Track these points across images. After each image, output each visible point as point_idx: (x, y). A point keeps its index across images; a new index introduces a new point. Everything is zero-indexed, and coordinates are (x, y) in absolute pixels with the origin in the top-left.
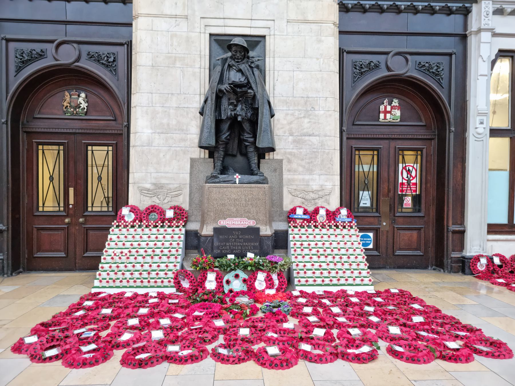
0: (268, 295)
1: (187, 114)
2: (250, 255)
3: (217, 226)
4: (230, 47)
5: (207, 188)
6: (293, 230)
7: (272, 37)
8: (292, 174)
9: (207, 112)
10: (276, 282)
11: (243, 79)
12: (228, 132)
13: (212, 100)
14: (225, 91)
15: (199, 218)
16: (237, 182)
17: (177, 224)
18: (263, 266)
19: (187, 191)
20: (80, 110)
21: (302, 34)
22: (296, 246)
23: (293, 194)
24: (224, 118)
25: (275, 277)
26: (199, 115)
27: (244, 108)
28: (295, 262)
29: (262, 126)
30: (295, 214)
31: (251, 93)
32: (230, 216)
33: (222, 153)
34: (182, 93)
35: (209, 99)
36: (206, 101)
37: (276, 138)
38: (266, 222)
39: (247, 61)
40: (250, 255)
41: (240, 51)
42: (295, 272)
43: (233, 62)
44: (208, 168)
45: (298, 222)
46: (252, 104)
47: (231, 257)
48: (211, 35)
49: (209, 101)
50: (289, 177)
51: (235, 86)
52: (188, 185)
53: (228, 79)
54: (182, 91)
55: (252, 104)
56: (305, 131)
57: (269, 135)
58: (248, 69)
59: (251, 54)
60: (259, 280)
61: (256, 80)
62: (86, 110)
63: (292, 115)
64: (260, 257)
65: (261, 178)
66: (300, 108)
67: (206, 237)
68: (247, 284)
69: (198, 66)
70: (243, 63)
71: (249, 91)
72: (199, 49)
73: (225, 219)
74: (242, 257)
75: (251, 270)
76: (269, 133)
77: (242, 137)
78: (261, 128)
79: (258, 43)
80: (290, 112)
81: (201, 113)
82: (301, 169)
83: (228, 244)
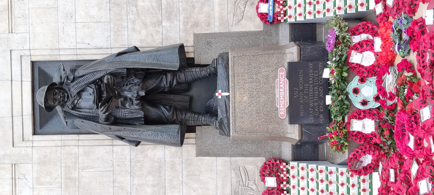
0: (383, 47)
1: (138, 161)
2: (326, 73)
3: (287, 119)
4: (49, 108)
5: (236, 135)
6: (290, 17)
7: (32, 52)
8: (212, 21)
9: (135, 136)
10: (364, 36)
11: (91, 90)
12: (160, 108)
13: (119, 130)
14: (107, 113)
15: (276, 143)
16: (227, 94)
17: (285, 173)
18: (341, 56)
19: (240, 160)
21: (27, 12)
22: (312, 11)
23: (240, 18)
24: (143, 113)
25: (356, 39)
26: (139, 147)
27: (128, 87)
28: (335, 12)
29: (151, 63)
30: (267, 14)
31: (108, 79)
32: (273, 101)
33: (189, 115)
34: (112, 169)
35: (118, 133)
36: (122, 138)
37: (167, 44)
38: (281, 53)
39: (67, 85)
40: (326, 73)
41: (54, 95)
42: (348, 12)
43: (68, 104)
44: (208, 133)
45: (279, 10)
46: (123, 78)
47: (329, 100)
48: (34, 133)
49: (121, 134)
50: (217, 24)
51: (99, 100)
52: (232, 158)
53: (92, 109)
54: (109, 169)
55: (123, 78)
56: (154, 4)
57: (162, 53)
58: (77, 84)
59: (56, 80)
60: (362, 61)
61: (91, 73)
63: (134, 22)
64: (328, 60)
65: (220, 62)
66: (124, 12)
67: (302, 133)
68: (367, 76)
69: (76, 150)
70: (69, 90)
71: (105, 81)
72: (54, 148)
73: (277, 109)
74: (329, 84)
75: (347, 71)
76: (159, 53)
77: (166, 90)
78: (154, 64)
79: (41, 71)
80: (130, 26)
81: (137, 143)
82: (206, 9)
83: (312, 105)
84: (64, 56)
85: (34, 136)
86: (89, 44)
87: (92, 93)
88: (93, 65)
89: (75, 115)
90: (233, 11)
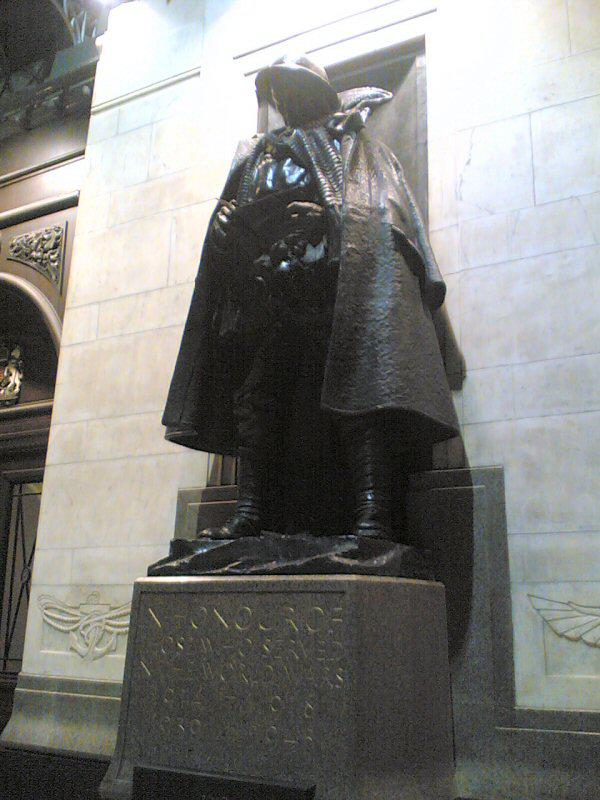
20: (8, 393)
23: (561, 626)
34: (171, 283)
62: (17, 389)
86: (468, 163)
90: (584, 604)
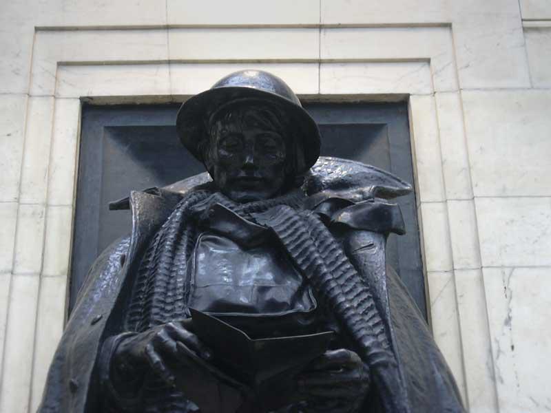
11: (284, 291)
14: (157, 358)
53: (185, 300)
58: (316, 234)
84: (441, 217)
85: (78, 102)
86: (508, 321)
87: (269, 296)
88: (415, 321)
89: (157, 227)
